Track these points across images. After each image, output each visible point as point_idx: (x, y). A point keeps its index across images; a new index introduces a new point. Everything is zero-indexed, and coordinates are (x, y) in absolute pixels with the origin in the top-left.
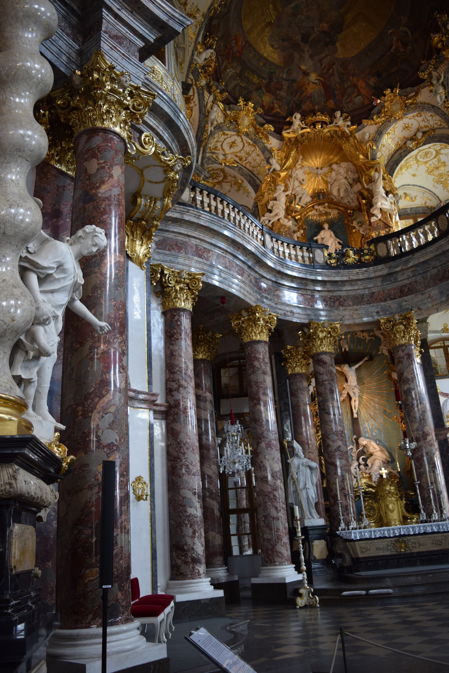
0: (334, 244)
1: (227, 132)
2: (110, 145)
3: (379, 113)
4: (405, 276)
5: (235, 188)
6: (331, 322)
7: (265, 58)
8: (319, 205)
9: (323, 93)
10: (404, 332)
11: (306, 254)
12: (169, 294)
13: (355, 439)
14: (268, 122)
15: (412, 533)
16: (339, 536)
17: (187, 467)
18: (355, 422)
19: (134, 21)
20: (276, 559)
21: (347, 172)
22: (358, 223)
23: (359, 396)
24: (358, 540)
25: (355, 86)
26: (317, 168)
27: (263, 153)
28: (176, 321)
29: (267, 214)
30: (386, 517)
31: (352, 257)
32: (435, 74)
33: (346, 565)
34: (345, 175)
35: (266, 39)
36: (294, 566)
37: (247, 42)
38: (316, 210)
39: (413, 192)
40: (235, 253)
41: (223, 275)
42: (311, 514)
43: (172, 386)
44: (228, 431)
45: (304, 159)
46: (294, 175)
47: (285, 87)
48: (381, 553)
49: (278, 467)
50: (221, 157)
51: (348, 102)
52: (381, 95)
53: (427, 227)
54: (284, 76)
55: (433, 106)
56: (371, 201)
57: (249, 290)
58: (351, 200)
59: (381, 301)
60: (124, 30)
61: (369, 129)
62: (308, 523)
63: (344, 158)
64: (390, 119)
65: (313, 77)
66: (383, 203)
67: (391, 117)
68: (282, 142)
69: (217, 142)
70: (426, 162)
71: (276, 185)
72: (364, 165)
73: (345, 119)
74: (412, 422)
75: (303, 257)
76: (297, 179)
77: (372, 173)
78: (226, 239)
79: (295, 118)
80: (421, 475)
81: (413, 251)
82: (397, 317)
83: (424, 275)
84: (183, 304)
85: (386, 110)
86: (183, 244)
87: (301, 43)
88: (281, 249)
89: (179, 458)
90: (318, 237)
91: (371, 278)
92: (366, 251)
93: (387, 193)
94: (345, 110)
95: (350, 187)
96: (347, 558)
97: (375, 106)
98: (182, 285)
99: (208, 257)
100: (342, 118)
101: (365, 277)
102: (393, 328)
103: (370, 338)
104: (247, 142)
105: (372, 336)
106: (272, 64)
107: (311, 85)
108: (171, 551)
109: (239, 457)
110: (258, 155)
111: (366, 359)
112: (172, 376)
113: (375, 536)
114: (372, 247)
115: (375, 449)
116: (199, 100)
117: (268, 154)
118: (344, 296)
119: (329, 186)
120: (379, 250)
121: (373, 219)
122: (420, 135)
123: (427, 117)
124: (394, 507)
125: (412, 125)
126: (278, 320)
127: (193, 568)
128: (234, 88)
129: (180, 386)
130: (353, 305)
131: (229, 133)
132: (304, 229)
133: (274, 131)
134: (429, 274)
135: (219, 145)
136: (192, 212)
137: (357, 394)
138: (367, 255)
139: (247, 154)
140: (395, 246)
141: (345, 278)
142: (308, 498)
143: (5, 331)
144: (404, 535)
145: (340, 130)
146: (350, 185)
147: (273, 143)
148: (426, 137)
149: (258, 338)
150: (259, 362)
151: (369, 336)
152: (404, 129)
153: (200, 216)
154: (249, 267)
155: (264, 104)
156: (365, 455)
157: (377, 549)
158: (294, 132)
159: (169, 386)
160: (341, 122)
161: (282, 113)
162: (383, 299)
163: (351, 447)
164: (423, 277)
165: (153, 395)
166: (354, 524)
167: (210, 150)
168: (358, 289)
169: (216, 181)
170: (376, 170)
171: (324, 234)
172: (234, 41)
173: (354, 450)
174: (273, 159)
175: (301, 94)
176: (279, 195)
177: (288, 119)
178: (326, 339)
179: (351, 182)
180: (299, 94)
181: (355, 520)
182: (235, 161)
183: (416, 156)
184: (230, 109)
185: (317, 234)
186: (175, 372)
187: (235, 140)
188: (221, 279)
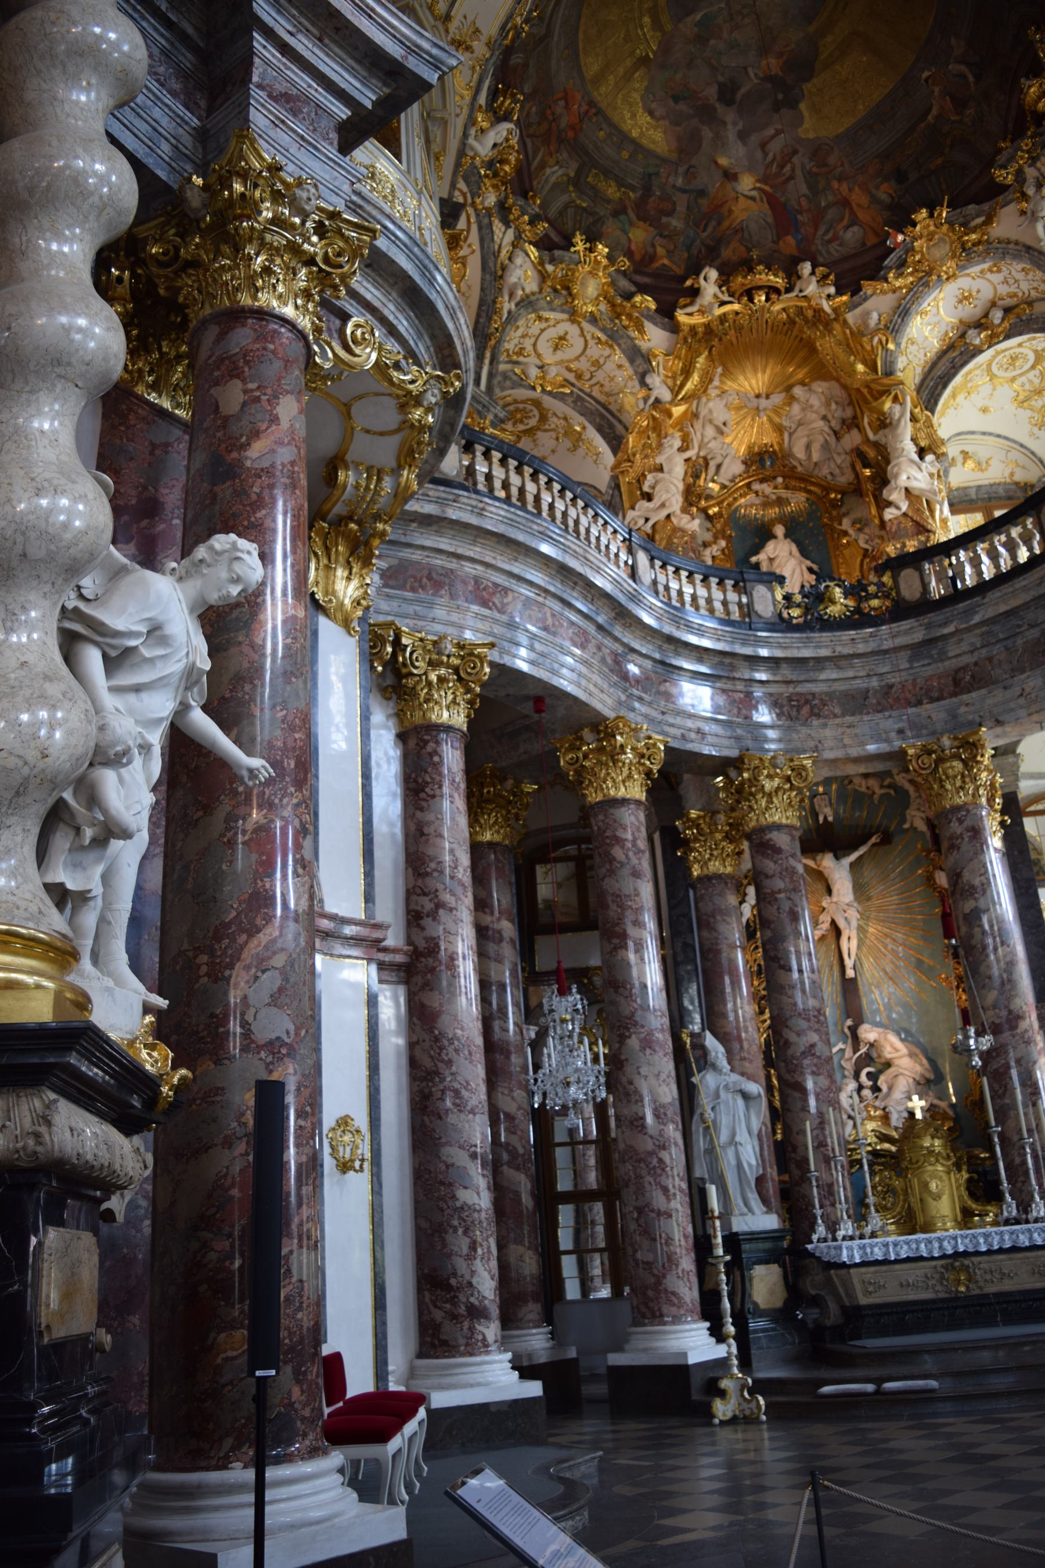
0: (798, 571)
1: (546, 314)
2: (271, 347)
3: (902, 264)
4: (965, 647)
5: (568, 444)
6: (792, 754)
7: (633, 141)
8: (762, 481)
9: (770, 220)
10: (963, 776)
11: (732, 596)
12: (413, 693)
13: (849, 1028)
14: (643, 289)
15: (984, 1249)
16: (812, 1255)
17: (457, 1093)
18: (849, 988)
19: (326, 59)
20: (666, 1309)
21: (828, 404)
22: (854, 523)
23: (860, 928)
24: (856, 1265)
25: (846, 203)
26: (758, 396)
27: (632, 361)
28: (431, 755)
29: (642, 505)
30: (923, 1210)
31: (840, 603)
32: (1030, 173)
33: (828, 1323)
34: (823, 412)
35: (636, 96)
36: (707, 1324)
37: (592, 104)
38: (757, 493)
39: (981, 448)
40: (565, 596)
41: (538, 646)
42: (746, 1204)
43: (420, 905)
44: (551, 1011)
45: (727, 373)
46: (703, 412)
47: (681, 208)
48: (912, 1296)
49: (669, 1093)
50: (534, 372)
51: (830, 241)
52: (904, 222)
53: (1015, 532)
54: (679, 182)
55: (1028, 248)
56: (885, 472)
57: (600, 681)
58: (837, 469)
59: (909, 704)
60: (303, 81)
61: (877, 303)
62: (740, 1224)
63: (821, 372)
64: (927, 279)
65: (747, 183)
66: (912, 475)
67: (929, 273)
68: (675, 336)
69: (523, 336)
70: (1013, 380)
71: (661, 435)
72: (868, 387)
73: (822, 281)
74: (984, 987)
75: (725, 603)
76: (711, 421)
77: (887, 405)
78: (546, 561)
79: (705, 279)
80: (1004, 1113)
81: (983, 587)
82: (946, 742)
83: (1009, 643)
84: (446, 714)
85: (917, 258)
86: (446, 575)
87: (717, 105)
88: (674, 585)
89: (437, 1073)
90: (762, 557)
91: (886, 652)
92: (872, 589)
93: (922, 453)
94: (821, 259)
95: (833, 439)
96: (833, 1307)
98: (443, 671)
99: (504, 605)
100: (814, 279)
101: (869, 650)
102: (937, 767)
103: (883, 791)
104: (593, 337)
105: (889, 786)
106: (648, 153)
107: (742, 202)
108: (420, 1290)
109: (577, 1070)
110: (620, 367)
111: (874, 840)
112: (420, 883)
113: (897, 1254)
114: (886, 579)
115: (897, 1051)
116: (482, 241)
117: (641, 362)
118: (821, 694)
119: (786, 436)
120: (902, 586)
121: (889, 514)
122: (997, 316)
123: (1014, 272)
124: (943, 1188)
125: (978, 291)
126: (669, 750)
127: (472, 1329)
128: (561, 213)
129: (439, 905)
130: (843, 715)
131: (551, 315)
132: (728, 539)
133: (656, 311)
134: (1020, 641)
135: (528, 343)
136: (465, 500)
137: (854, 923)
138: (876, 597)
139: (593, 365)
140: (940, 577)
141: (824, 652)
142: (739, 1165)
143: (25, 782)
144: (965, 1254)
145: (810, 307)
146: (835, 433)
147: (654, 337)
148: (1012, 318)
149: (622, 793)
150: (623, 847)
151: (882, 787)
152: (960, 302)
153: (483, 509)
154: (600, 628)
155: (633, 247)
156: (873, 1064)
157: (901, 1285)
158: (702, 312)
159: (413, 907)
160: (812, 288)
161: (674, 267)
162: (913, 700)
163: (841, 1046)
164: (1007, 649)
165: (377, 926)
166: (847, 1228)
167: (508, 355)
168: (855, 678)
169: (521, 427)
170: (896, 400)
171: (775, 549)
172: (562, 103)
173: (849, 1053)
174: (655, 376)
175: (719, 223)
176: (669, 459)
177: (688, 283)
178: (780, 793)
179: (837, 428)
180: (713, 223)
181: (849, 1217)
182: (566, 380)
183: (989, 365)
184: (552, 260)
185: (757, 549)
186: (427, 874)
187: (566, 333)
188: (533, 656)
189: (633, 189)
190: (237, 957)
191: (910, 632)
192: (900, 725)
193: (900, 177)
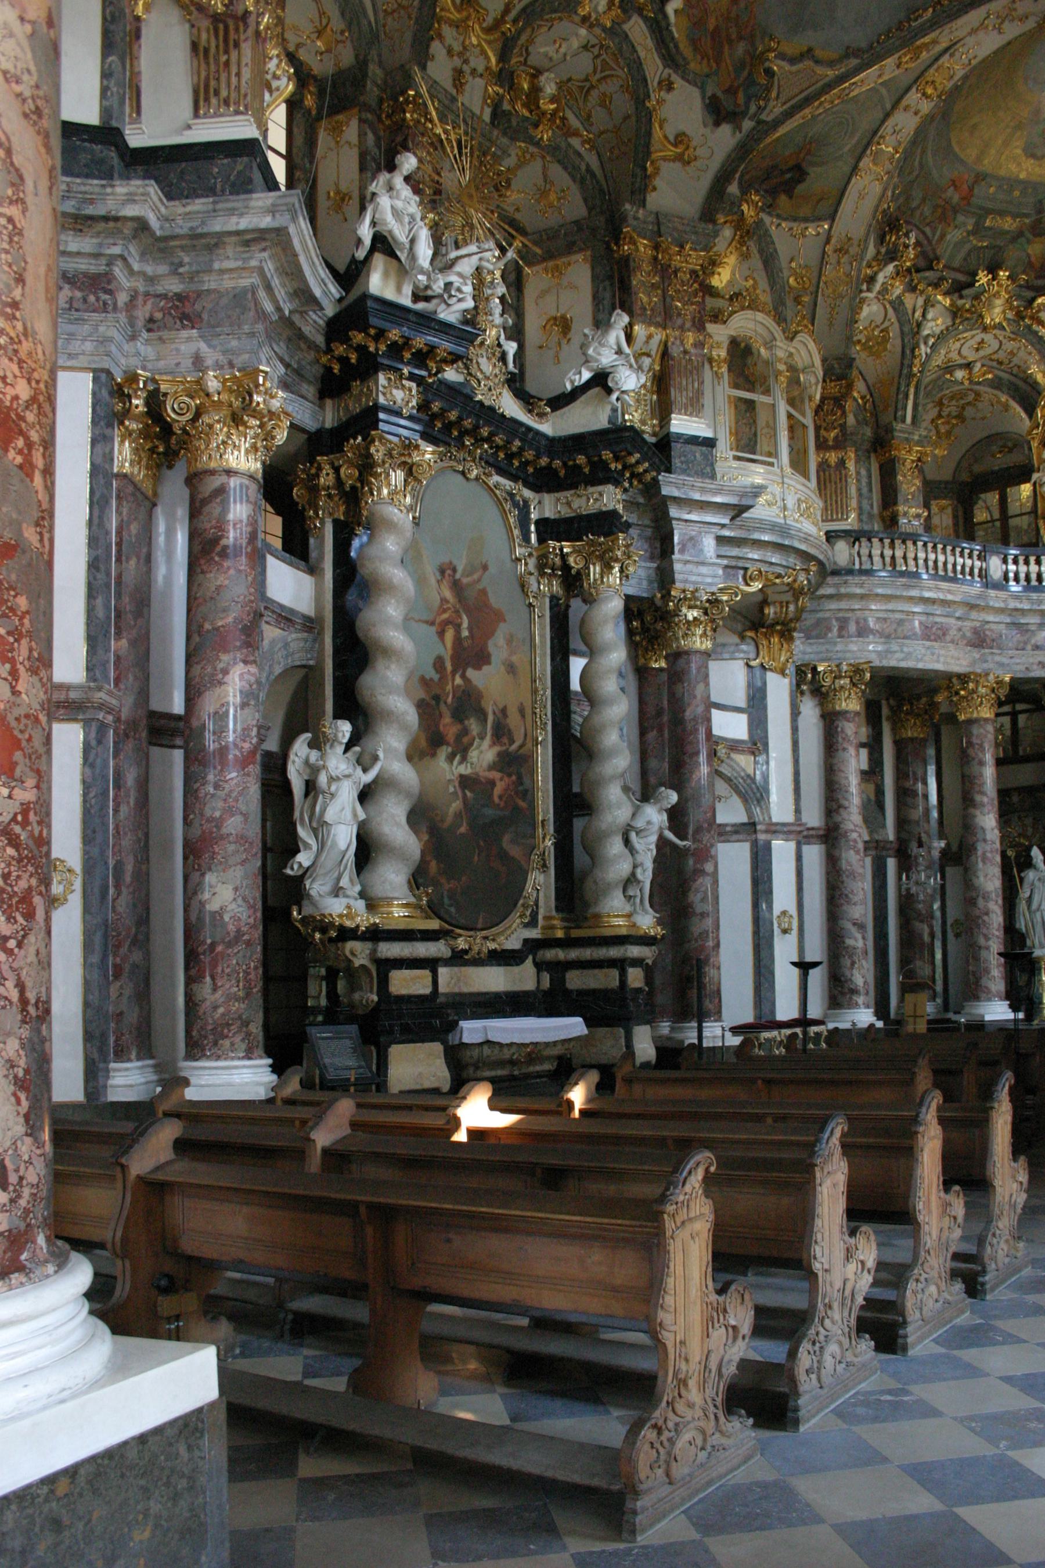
129: (840, 806)
154: (959, 618)
155: (1033, 259)
184: (961, 297)
189: (1026, 216)
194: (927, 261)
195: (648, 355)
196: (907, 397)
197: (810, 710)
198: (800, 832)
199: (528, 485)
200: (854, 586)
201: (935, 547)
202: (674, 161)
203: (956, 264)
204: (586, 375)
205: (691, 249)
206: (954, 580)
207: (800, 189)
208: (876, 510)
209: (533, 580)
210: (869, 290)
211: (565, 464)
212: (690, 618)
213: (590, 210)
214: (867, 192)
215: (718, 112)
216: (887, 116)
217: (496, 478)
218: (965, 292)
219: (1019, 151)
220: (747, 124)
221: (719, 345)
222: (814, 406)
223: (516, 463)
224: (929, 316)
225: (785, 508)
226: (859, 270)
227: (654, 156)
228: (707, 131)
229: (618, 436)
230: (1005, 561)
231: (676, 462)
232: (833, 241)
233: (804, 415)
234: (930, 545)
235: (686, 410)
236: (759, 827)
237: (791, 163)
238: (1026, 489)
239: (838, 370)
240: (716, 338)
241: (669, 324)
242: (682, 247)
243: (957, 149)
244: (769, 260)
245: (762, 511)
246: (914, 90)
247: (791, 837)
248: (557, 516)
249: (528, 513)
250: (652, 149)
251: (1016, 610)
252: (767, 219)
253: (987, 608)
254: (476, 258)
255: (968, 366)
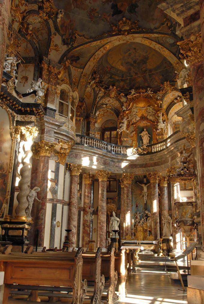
14: (122, 92)
37: (112, 67)
43: (70, 197)
45: (136, 104)
84: (76, 173)
90: (141, 134)
93: (164, 121)
97: (161, 87)
137: (146, 195)
147: (123, 99)
154: (101, 158)
165: (64, 200)
184: (106, 90)
185: (141, 132)
190: (40, 212)
191: (148, 157)
192: (147, 170)
193: (163, 76)
194: (100, 82)
195: (44, 89)
196: (94, 109)
197: (68, 174)
198: (64, 202)
199: (15, 112)
200: (80, 147)
201: (97, 141)
202: (55, 50)
203: (106, 83)
204: (32, 91)
205: (56, 69)
206: (101, 149)
207: (78, 61)
208: (85, 132)
209: (13, 134)
210: (89, 85)
211: (24, 109)
212: (46, 148)
213: (36, 55)
214: (91, 65)
215: (64, 42)
216: (97, 51)
217: (9, 109)
218: (107, 89)
219: (120, 64)
220: (70, 46)
221: (58, 90)
222: (76, 107)
223: (14, 107)
224: (100, 93)
225: (69, 128)
226: (88, 80)
227: (50, 48)
228: (62, 46)
229: (36, 105)
230: (111, 147)
231: (47, 113)
232: (83, 73)
233: (74, 109)
234: (97, 141)
235: (51, 102)
236: (54, 200)
237: (77, 56)
238: (115, 132)
239: (82, 100)
240: (59, 89)
241: (49, 83)
242: (54, 68)
243: (109, 61)
244: (70, 75)
245: (64, 128)
246: (102, 48)
247: (61, 203)
248: (21, 120)
249: (15, 118)
250: (50, 46)
251: (113, 158)
252: (70, 66)
253: (107, 157)
254: (12, 60)
255: (106, 104)
